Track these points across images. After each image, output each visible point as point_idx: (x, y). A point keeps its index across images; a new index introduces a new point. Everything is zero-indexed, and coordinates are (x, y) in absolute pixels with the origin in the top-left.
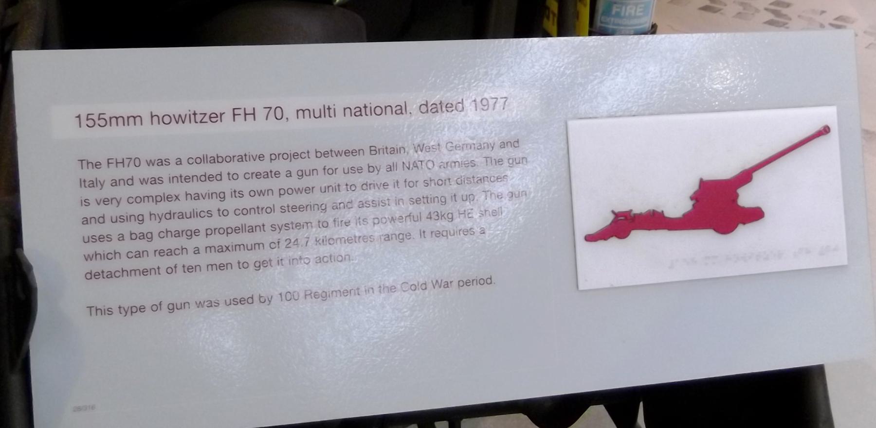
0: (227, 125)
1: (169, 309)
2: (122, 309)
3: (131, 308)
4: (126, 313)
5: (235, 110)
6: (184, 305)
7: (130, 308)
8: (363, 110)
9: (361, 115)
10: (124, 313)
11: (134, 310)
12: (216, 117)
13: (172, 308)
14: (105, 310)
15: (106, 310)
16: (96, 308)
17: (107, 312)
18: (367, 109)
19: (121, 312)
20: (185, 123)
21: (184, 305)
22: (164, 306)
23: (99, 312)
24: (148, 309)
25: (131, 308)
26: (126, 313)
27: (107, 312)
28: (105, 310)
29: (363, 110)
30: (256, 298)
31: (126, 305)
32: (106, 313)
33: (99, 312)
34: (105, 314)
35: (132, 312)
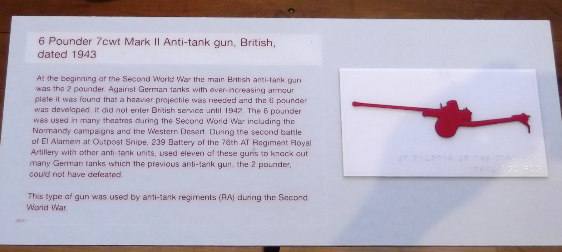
1: (76, 199)
2: (48, 196)
3: (54, 196)
4: (50, 199)
5: (242, 40)
6: (85, 197)
10: (49, 199)
11: (55, 197)
13: (78, 198)
15: (39, 196)
17: (39, 197)
21: (85, 197)
24: (63, 197)
25: (54, 196)
32: (39, 198)
33: (35, 196)
34: (38, 198)
35: (54, 198)
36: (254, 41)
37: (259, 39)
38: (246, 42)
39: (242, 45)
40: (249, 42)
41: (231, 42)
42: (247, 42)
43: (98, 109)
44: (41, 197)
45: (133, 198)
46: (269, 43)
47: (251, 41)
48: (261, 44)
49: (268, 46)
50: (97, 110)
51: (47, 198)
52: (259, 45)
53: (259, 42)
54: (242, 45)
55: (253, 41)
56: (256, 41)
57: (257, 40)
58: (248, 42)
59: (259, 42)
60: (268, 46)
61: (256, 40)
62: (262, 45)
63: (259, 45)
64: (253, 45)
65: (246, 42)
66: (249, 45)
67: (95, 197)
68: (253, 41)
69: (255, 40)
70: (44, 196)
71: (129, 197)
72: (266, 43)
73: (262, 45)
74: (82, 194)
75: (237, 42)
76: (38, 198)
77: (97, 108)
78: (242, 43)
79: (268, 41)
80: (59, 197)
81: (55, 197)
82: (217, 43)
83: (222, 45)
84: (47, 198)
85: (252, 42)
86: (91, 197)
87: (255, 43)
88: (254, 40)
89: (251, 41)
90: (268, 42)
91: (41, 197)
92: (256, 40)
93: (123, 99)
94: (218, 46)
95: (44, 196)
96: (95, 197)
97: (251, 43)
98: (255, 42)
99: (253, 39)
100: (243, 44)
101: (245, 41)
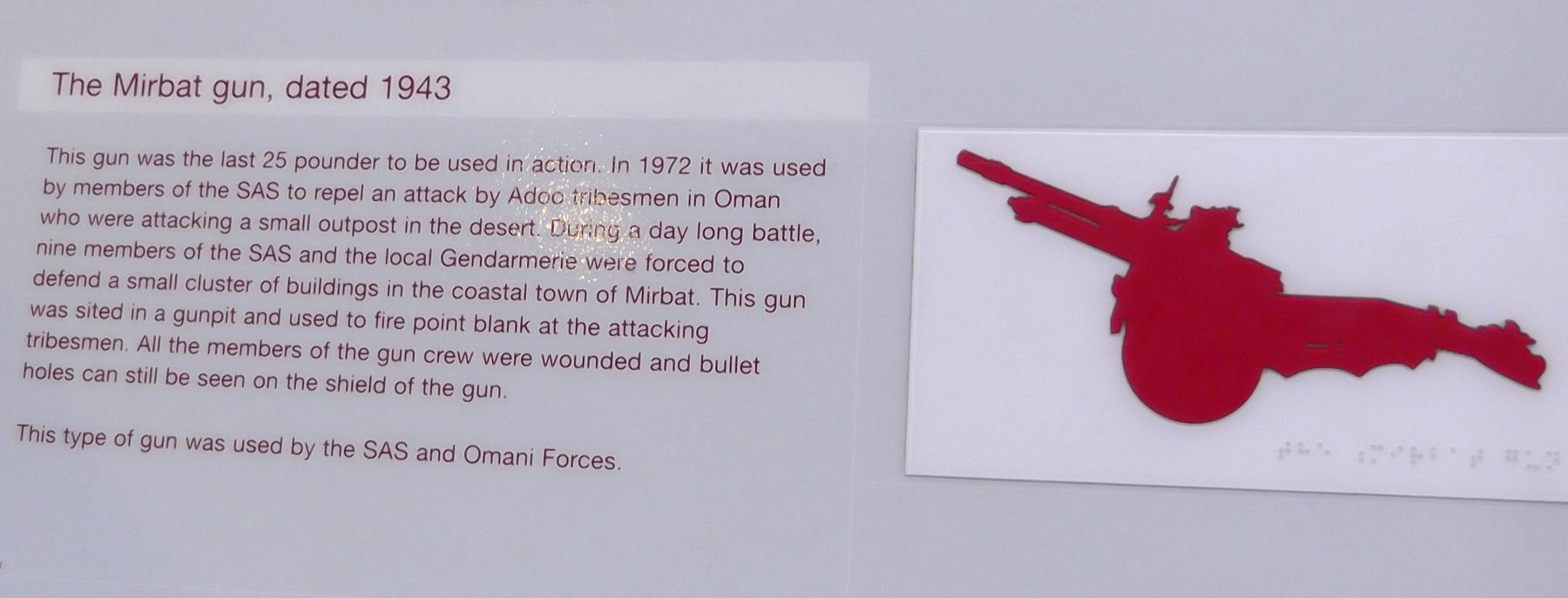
0: (202, 104)
2: (69, 435)
3: (85, 435)
6: (168, 441)
7: (82, 435)
8: (322, 87)
9: (317, 96)
11: (88, 438)
12: (188, 88)
13: (149, 444)
15: (45, 434)
17: (46, 437)
18: (328, 85)
20: (128, 95)
21: (168, 441)
22: (136, 440)
23: (34, 435)
25: (85, 435)
26: (75, 442)
27: (46, 437)
29: (322, 87)
30: (287, 445)
31: (77, 429)
33: (34, 435)
35: (84, 442)
41: (260, 85)
67: (192, 444)
70: (59, 436)
74: (159, 433)
81: (88, 438)
86: (182, 444)
93: (249, 219)
95: (59, 436)
96: (192, 444)
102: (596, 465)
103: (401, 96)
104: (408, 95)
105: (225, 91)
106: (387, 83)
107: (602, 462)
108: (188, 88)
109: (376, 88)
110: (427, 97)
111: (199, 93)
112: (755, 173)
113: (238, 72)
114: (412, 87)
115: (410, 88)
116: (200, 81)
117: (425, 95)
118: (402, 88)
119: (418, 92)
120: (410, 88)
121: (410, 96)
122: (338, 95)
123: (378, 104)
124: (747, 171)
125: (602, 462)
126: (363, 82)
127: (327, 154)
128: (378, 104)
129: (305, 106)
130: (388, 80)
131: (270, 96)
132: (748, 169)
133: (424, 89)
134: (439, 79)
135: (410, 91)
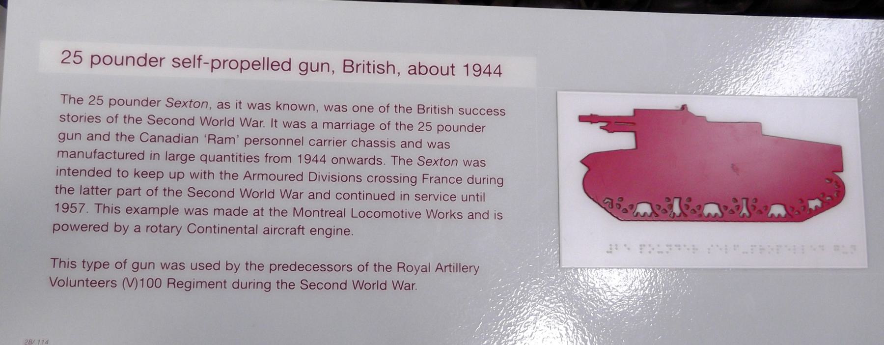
3: (95, 263)
7: (94, 263)
11: (98, 265)
14: (68, 262)
16: (60, 260)
19: (85, 266)
22: (129, 265)
25: (95, 263)
26: (90, 267)
28: (68, 262)
34: (68, 267)
35: (95, 267)
36: (365, 65)
37: (374, 61)
38: (351, 66)
39: (346, 70)
40: (357, 66)
42: (353, 66)
43: (276, 121)
44: (73, 265)
45: (229, 267)
46: (391, 68)
47: (360, 64)
48: (376, 69)
49: (388, 73)
50: (274, 123)
51: (84, 267)
52: (374, 72)
53: (374, 65)
54: (344, 71)
55: (364, 65)
56: (368, 64)
57: (370, 63)
58: (356, 66)
59: (374, 65)
60: (388, 73)
61: (368, 62)
62: (378, 72)
63: (374, 72)
64: (364, 72)
65: (351, 66)
66: (357, 72)
68: (364, 65)
69: (367, 63)
70: (79, 264)
71: (223, 266)
72: (385, 69)
73: (378, 72)
75: (337, 66)
76: (68, 267)
77: (274, 120)
78: (346, 67)
79: (389, 64)
80: (105, 265)
82: (303, 67)
83: (312, 71)
84: (84, 267)
85: (362, 65)
87: (366, 67)
88: (366, 63)
89: (360, 64)
90: (388, 66)
91: (73, 265)
92: (368, 62)
94: (305, 72)
95: (79, 264)
97: (360, 68)
98: (367, 66)
99: (364, 61)
100: (347, 69)
101: (350, 63)
102: (315, 269)
103: (474, 75)
104: (478, 74)
105: (306, 68)
106: (466, 68)
107: (318, 267)
108: (349, 66)
109: (460, 70)
110: (489, 76)
111: (454, 74)
112: (343, 111)
113: (314, 57)
114: (480, 70)
115: (479, 71)
116: (454, 67)
117: (488, 74)
118: (474, 70)
119: (484, 73)
120: (479, 71)
121: (479, 75)
122: (185, 66)
123: (461, 78)
124: (338, 109)
125: (318, 267)
126: (289, 61)
127: (129, 97)
128: (461, 78)
129: (181, 72)
130: (467, 66)
131: (399, 73)
132: (338, 109)
133: (487, 71)
134: (63, 52)
135: (479, 72)
